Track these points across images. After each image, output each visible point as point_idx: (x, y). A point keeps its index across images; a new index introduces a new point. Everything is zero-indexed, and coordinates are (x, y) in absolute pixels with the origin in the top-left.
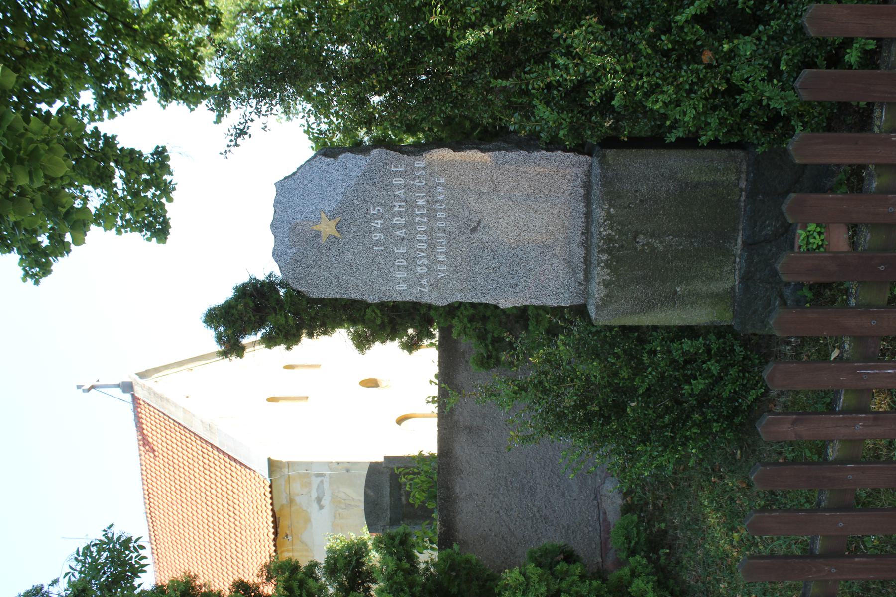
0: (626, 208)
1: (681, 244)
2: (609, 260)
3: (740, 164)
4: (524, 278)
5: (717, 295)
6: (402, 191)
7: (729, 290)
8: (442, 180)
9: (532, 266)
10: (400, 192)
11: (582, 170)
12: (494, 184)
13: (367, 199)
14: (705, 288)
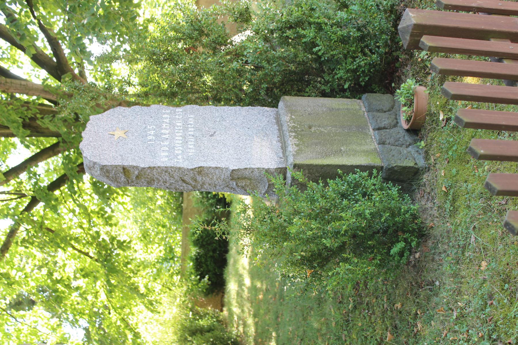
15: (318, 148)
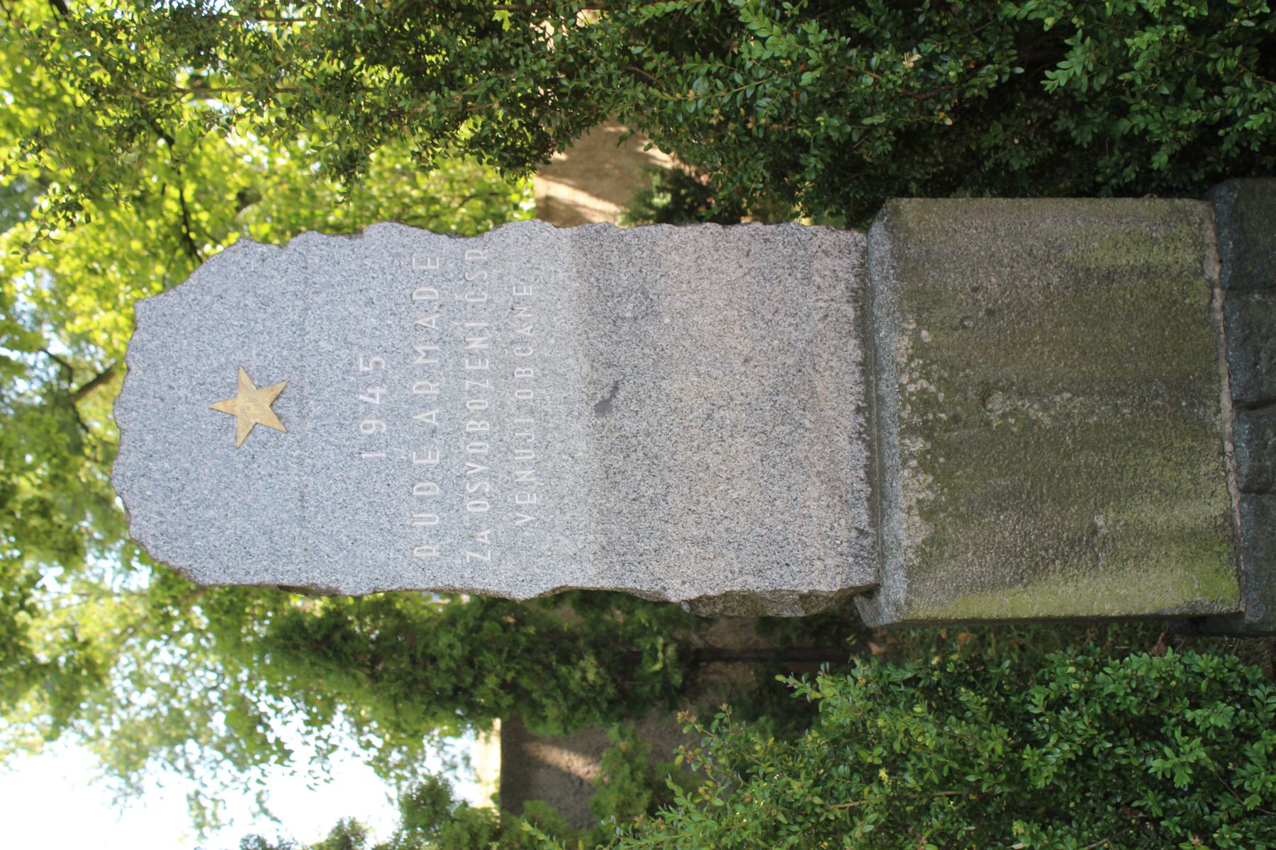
0: (956, 329)
2: (928, 452)
3: (1200, 229)
4: (726, 522)
5: (1193, 534)
6: (434, 318)
7: (1220, 521)
8: (527, 291)
9: (744, 493)
10: (430, 321)
11: (846, 262)
12: (647, 297)
13: (352, 337)
14: (1161, 519)
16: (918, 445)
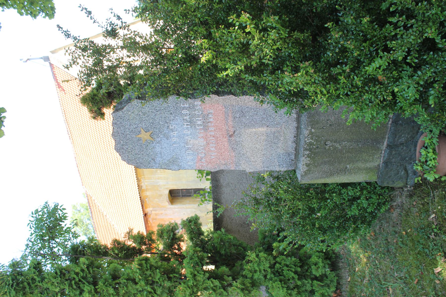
1: (352, 146)
5: (370, 168)
8: (211, 111)
9: (265, 153)
13: (167, 121)
15: (326, 168)
16: (308, 152)
